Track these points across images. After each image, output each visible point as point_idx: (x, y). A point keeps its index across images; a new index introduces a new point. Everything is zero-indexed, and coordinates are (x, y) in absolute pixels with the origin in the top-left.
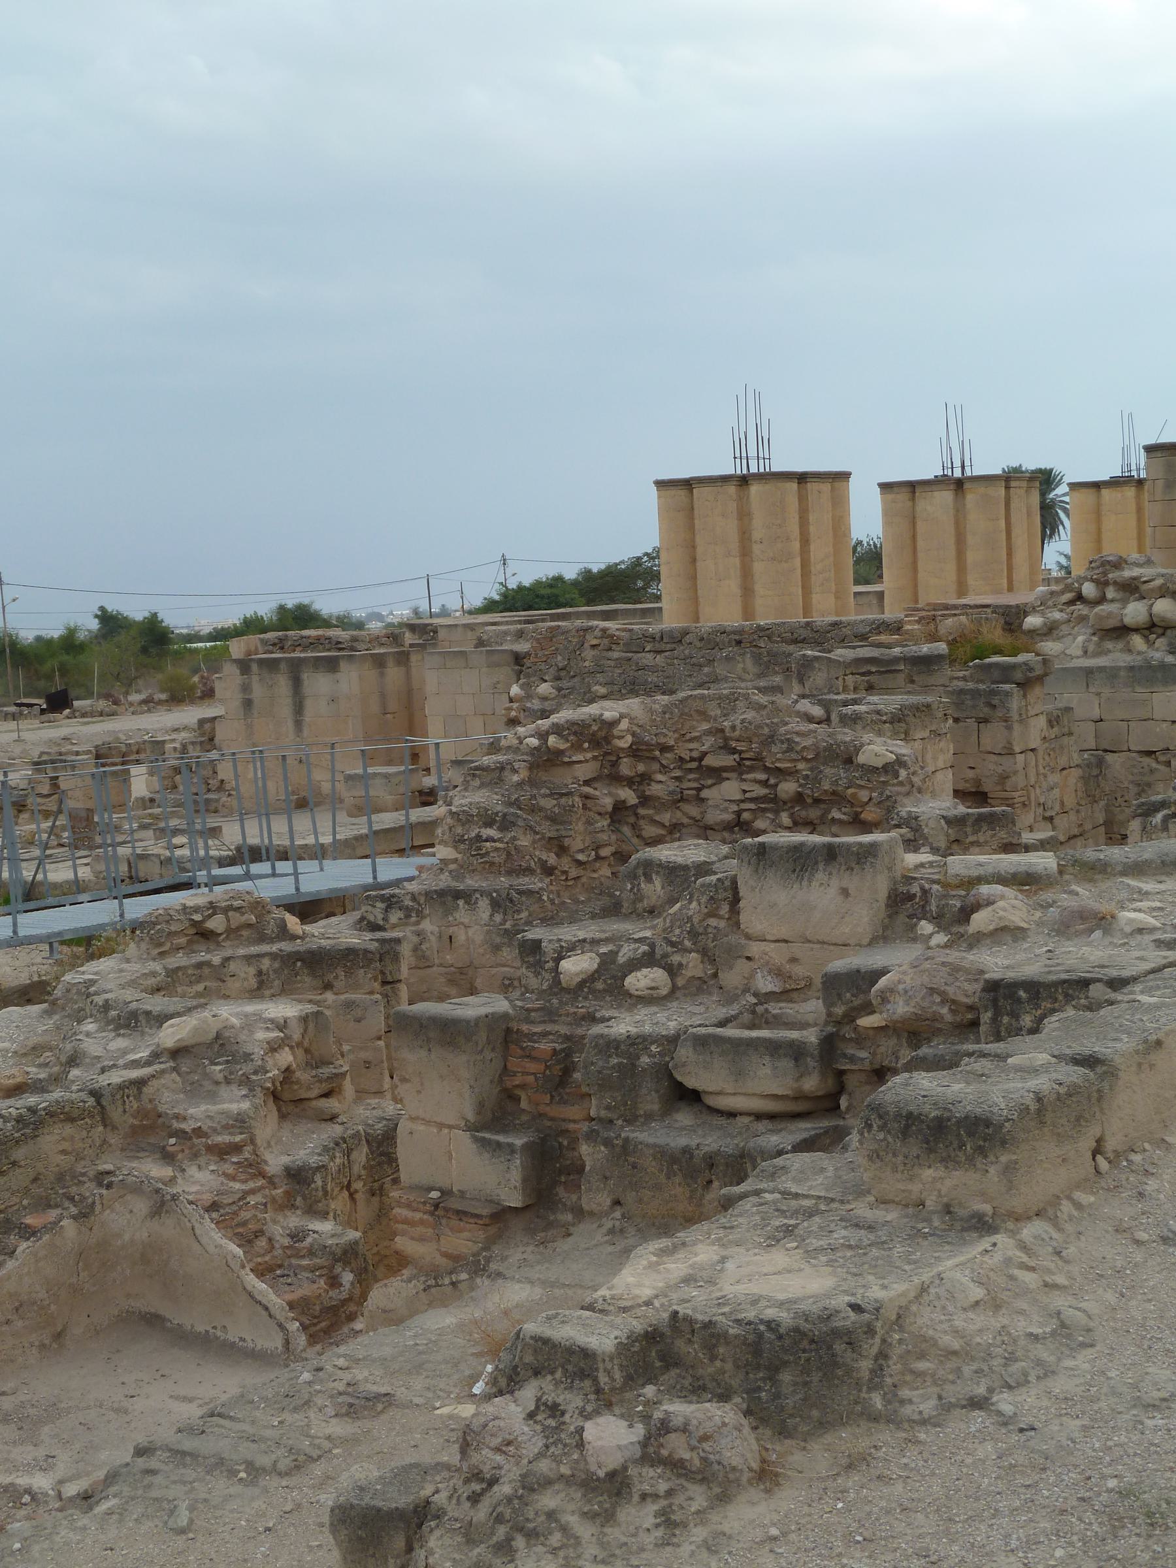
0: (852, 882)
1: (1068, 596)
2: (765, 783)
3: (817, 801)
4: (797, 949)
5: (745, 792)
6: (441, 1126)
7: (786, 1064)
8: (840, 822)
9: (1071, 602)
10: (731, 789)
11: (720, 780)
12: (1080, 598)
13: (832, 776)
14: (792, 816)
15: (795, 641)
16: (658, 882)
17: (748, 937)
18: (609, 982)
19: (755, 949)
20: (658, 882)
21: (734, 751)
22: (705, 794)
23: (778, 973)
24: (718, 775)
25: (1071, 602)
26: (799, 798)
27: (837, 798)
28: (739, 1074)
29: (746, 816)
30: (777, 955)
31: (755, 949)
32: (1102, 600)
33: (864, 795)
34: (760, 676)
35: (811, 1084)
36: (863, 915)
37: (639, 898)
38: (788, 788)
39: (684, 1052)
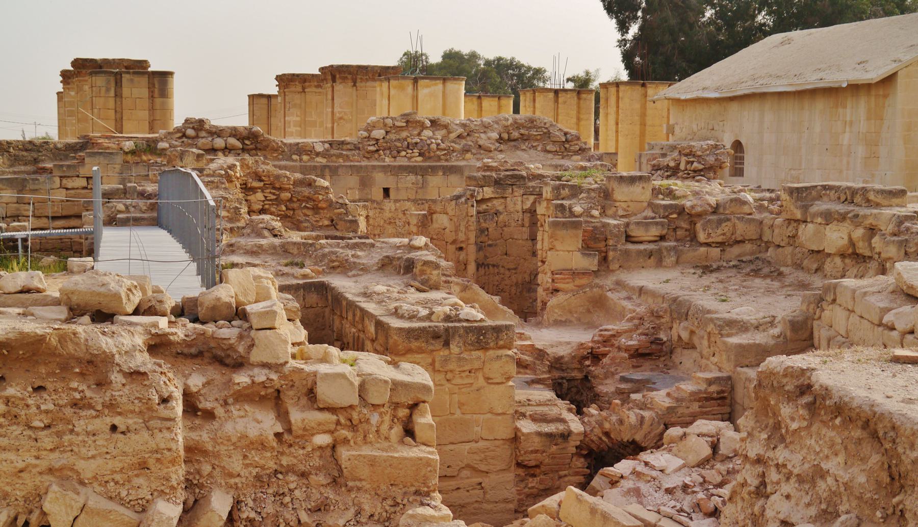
0: (645, 185)
1: (179, 135)
2: (274, 194)
3: (299, 200)
4: (630, 204)
5: (266, 197)
6: (569, 251)
7: (660, 227)
8: (308, 208)
9: (180, 138)
10: (260, 196)
11: (255, 193)
12: (184, 135)
13: (306, 191)
14: (286, 206)
15: (26, 150)
16: (567, 190)
17: (615, 201)
18: (587, 213)
19: (617, 204)
20: (567, 190)
21: (261, 180)
22: (249, 198)
23: (625, 210)
24: (253, 190)
25: (180, 138)
26: (290, 200)
27: (309, 199)
28: (647, 231)
29: (267, 206)
30: (624, 205)
31: (617, 204)
32: (197, 137)
33: (321, 197)
34: (11, 166)
35: (664, 232)
36: (647, 195)
37: (560, 194)
38: (286, 195)
39: (632, 227)
